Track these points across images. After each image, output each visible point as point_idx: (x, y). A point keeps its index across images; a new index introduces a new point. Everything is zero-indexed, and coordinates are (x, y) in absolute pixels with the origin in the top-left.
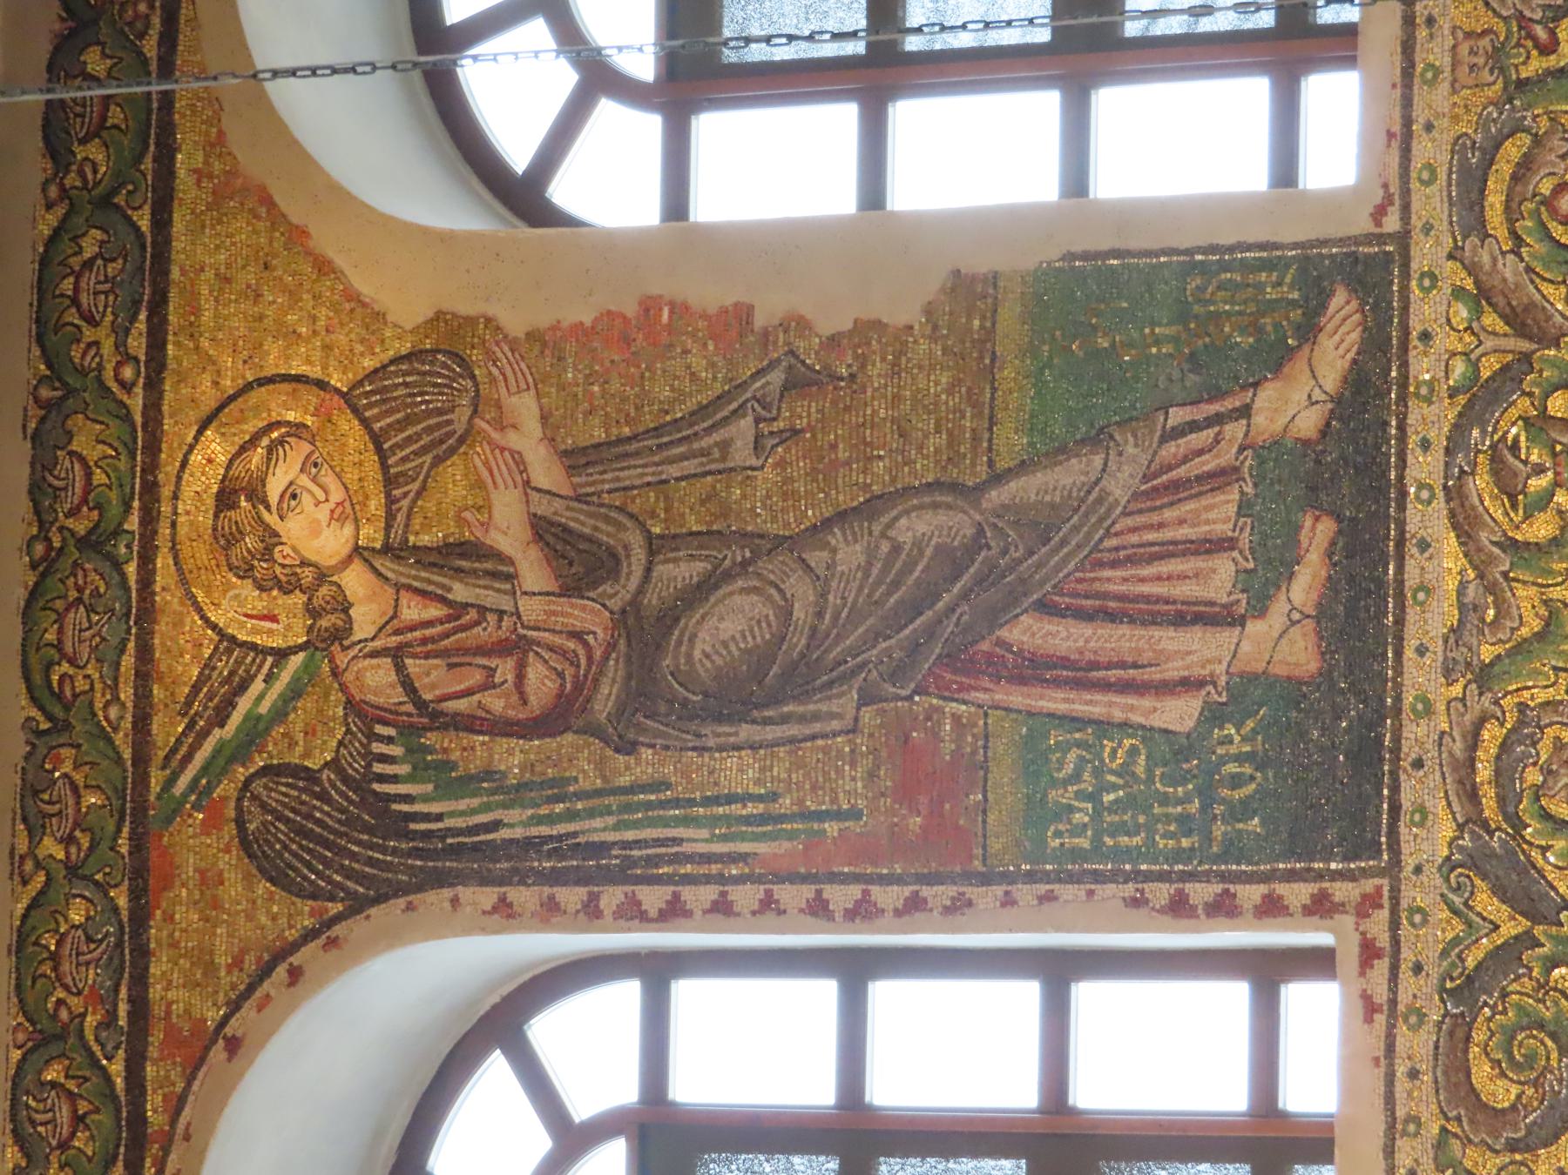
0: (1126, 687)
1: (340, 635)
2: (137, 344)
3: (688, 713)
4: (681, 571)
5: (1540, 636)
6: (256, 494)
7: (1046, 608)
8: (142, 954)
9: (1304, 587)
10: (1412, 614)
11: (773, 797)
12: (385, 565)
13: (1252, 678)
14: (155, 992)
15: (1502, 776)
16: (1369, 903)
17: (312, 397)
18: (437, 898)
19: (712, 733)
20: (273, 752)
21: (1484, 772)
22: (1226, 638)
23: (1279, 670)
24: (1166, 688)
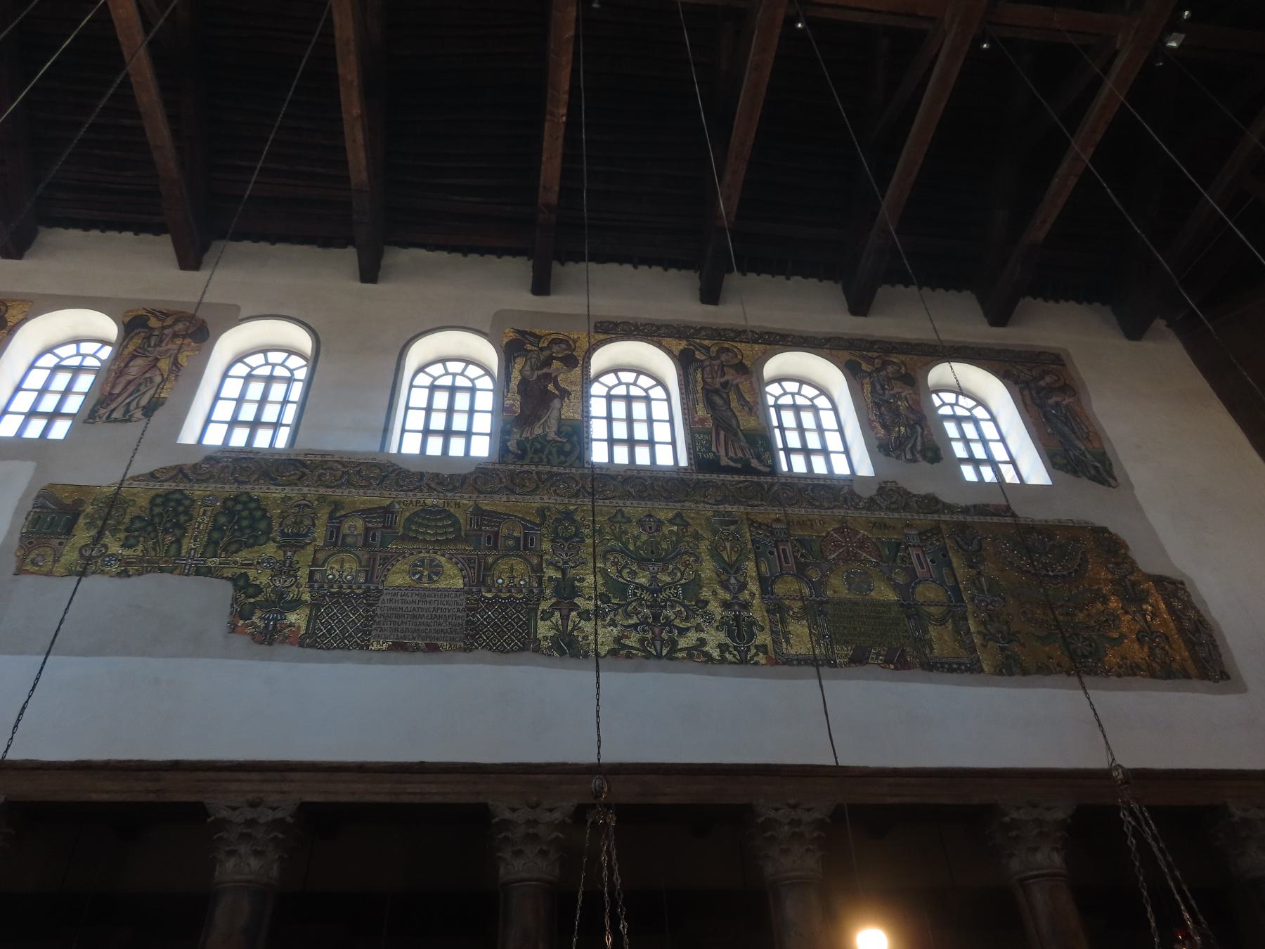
0: (716, 445)
1: (712, 360)
3: (707, 395)
4: (725, 396)
7: (725, 436)
9: (732, 464)
16: (693, 470)
18: (681, 368)
20: (697, 353)
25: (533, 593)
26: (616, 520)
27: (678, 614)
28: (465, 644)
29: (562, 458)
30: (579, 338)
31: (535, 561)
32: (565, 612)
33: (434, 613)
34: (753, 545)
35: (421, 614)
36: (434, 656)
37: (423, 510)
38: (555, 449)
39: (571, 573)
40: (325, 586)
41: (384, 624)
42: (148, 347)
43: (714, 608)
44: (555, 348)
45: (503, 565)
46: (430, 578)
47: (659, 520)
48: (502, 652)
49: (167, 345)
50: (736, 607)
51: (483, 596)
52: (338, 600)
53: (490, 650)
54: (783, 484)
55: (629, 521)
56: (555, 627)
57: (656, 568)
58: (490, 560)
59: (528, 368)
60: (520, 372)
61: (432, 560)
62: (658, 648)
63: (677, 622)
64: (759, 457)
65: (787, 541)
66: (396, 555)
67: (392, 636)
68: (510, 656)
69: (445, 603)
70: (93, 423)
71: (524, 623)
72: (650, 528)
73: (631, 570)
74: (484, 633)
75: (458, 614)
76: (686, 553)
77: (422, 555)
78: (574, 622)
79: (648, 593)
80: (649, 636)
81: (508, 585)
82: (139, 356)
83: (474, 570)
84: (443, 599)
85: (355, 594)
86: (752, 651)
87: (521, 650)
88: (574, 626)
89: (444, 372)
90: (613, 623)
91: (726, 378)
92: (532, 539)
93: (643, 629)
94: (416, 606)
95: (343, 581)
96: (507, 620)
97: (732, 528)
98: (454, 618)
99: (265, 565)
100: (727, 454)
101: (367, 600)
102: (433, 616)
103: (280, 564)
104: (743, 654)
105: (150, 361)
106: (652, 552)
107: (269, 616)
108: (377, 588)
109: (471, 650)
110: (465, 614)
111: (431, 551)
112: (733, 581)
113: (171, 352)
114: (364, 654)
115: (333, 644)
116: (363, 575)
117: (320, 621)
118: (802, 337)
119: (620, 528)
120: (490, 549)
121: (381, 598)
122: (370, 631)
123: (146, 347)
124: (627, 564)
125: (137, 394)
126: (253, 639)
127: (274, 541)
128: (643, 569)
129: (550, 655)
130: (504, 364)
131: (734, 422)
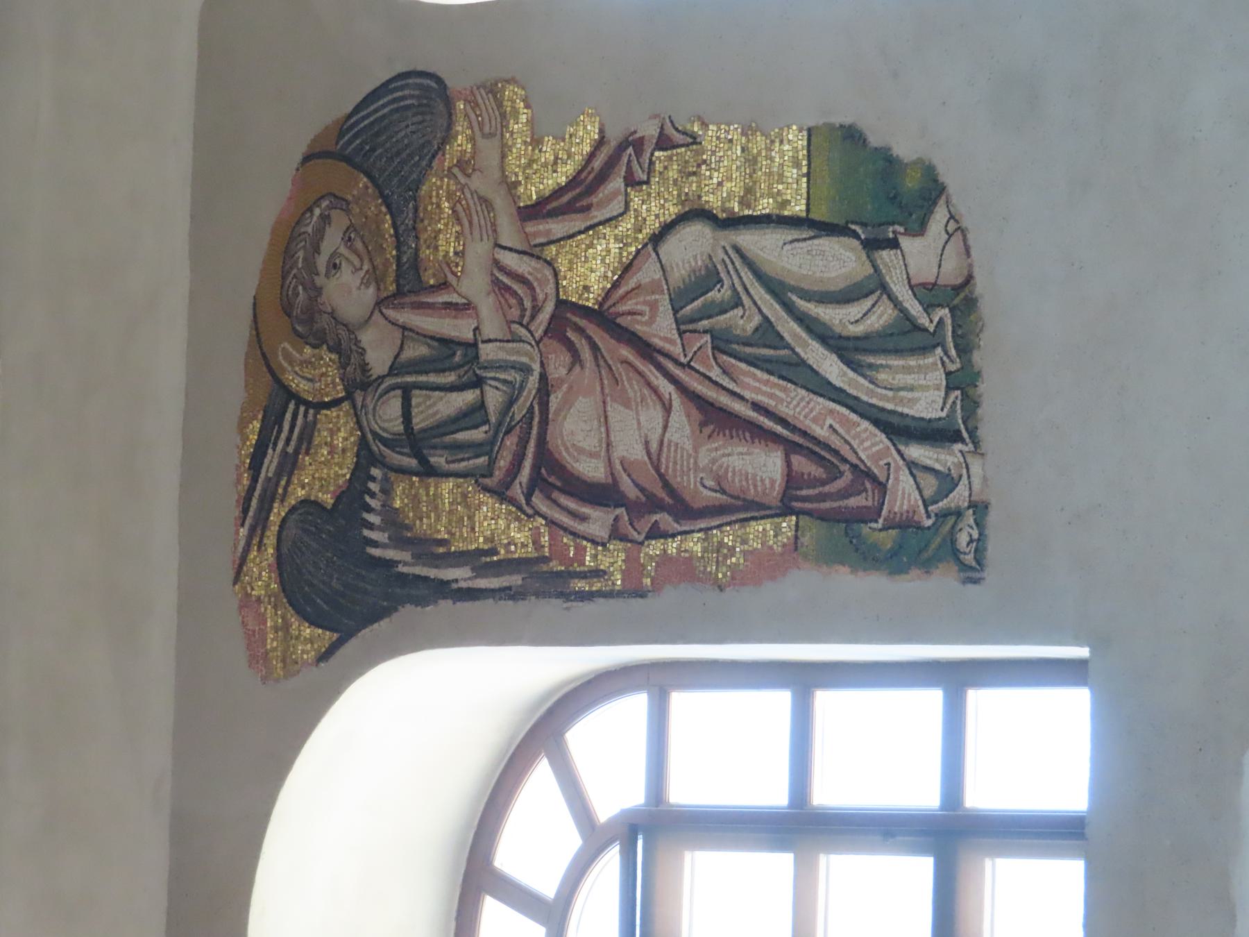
42: (486, 421)
49: (464, 308)
70: (980, 508)
82: (542, 441)
105: (576, 358)
113: (509, 260)
123: (478, 435)
125: (789, 328)
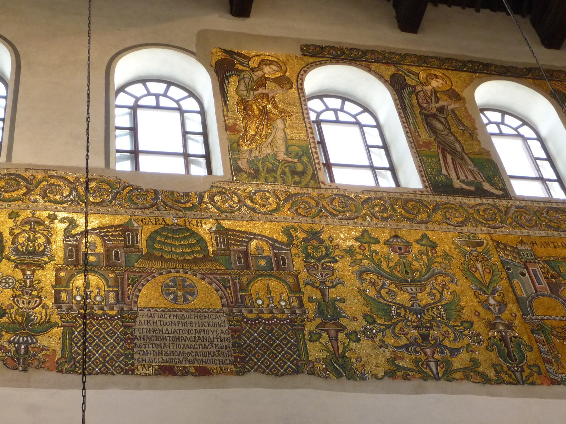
2: (449, 68)
4: (443, 121)
5: (469, 213)
6: (437, 78)
7: (452, 159)
8: (378, 63)
9: (464, 186)
10: (466, 198)
11: (419, 128)
12: (433, 90)
13: (452, 180)
14: (374, 64)
15: (450, 207)
16: (428, 192)
17: (450, 84)
18: (395, 93)
19: (424, 122)
21: (449, 205)
22: (456, 178)
23: (454, 183)
24: (447, 171)
25: (296, 314)
26: (364, 241)
27: (446, 335)
28: (236, 367)
29: (297, 178)
30: (288, 60)
31: (291, 281)
32: (333, 333)
33: (197, 335)
34: (504, 266)
35: (184, 336)
36: (204, 380)
37: (163, 229)
38: (287, 168)
39: (332, 294)
40: (74, 307)
41: (145, 347)
43: (479, 327)
44: (267, 69)
45: (258, 285)
46: (186, 299)
47: (408, 242)
48: (276, 375)
50: (501, 328)
51: (244, 317)
52: (91, 322)
53: (263, 373)
54: (517, 207)
55: (377, 241)
56: (325, 348)
57: (414, 289)
58: (244, 280)
59: (242, 87)
60: (237, 91)
61: (184, 281)
62: (434, 369)
63: (446, 343)
64: (489, 180)
65: (535, 262)
66: (145, 275)
67: (157, 360)
68: (286, 378)
69: (206, 324)
71: (293, 345)
72: (400, 248)
73: (390, 290)
74: (254, 355)
75: (223, 336)
76: (440, 274)
77: (172, 275)
78: (344, 343)
79: (412, 314)
80: (423, 357)
81: (268, 305)
83: (230, 290)
84: (203, 321)
85: (108, 315)
86: (526, 371)
87: (297, 372)
88: (345, 347)
89: (146, 92)
90: (383, 344)
91: (441, 103)
92: (283, 259)
93: (415, 349)
94: (176, 328)
95: (93, 302)
96: (274, 342)
97: (480, 249)
98: (219, 340)
99: (4, 284)
100: (458, 178)
101: (122, 322)
102: (197, 338)
103: (21, 284)
104: (518, 374)
106: (407, 273)
107: (19, 339)
108: (131, 309)
109: (244, 374)
110: (230, 336)
111: (181, 271)
112: (492, 301)
114: (129, 378)
115: (94, 369)
116: (112, 294)
117: (76, 344)
118: (504, 67)
119: (370, 247)
120: (242, 269)
121: (138, 320)
122: (133, 355)
124: (384, 284)
126: (5, 364)
127: (9, 259)
128: (402, 290)
129: (327, 377)
130: (218, 83)
131: (457, 146)
